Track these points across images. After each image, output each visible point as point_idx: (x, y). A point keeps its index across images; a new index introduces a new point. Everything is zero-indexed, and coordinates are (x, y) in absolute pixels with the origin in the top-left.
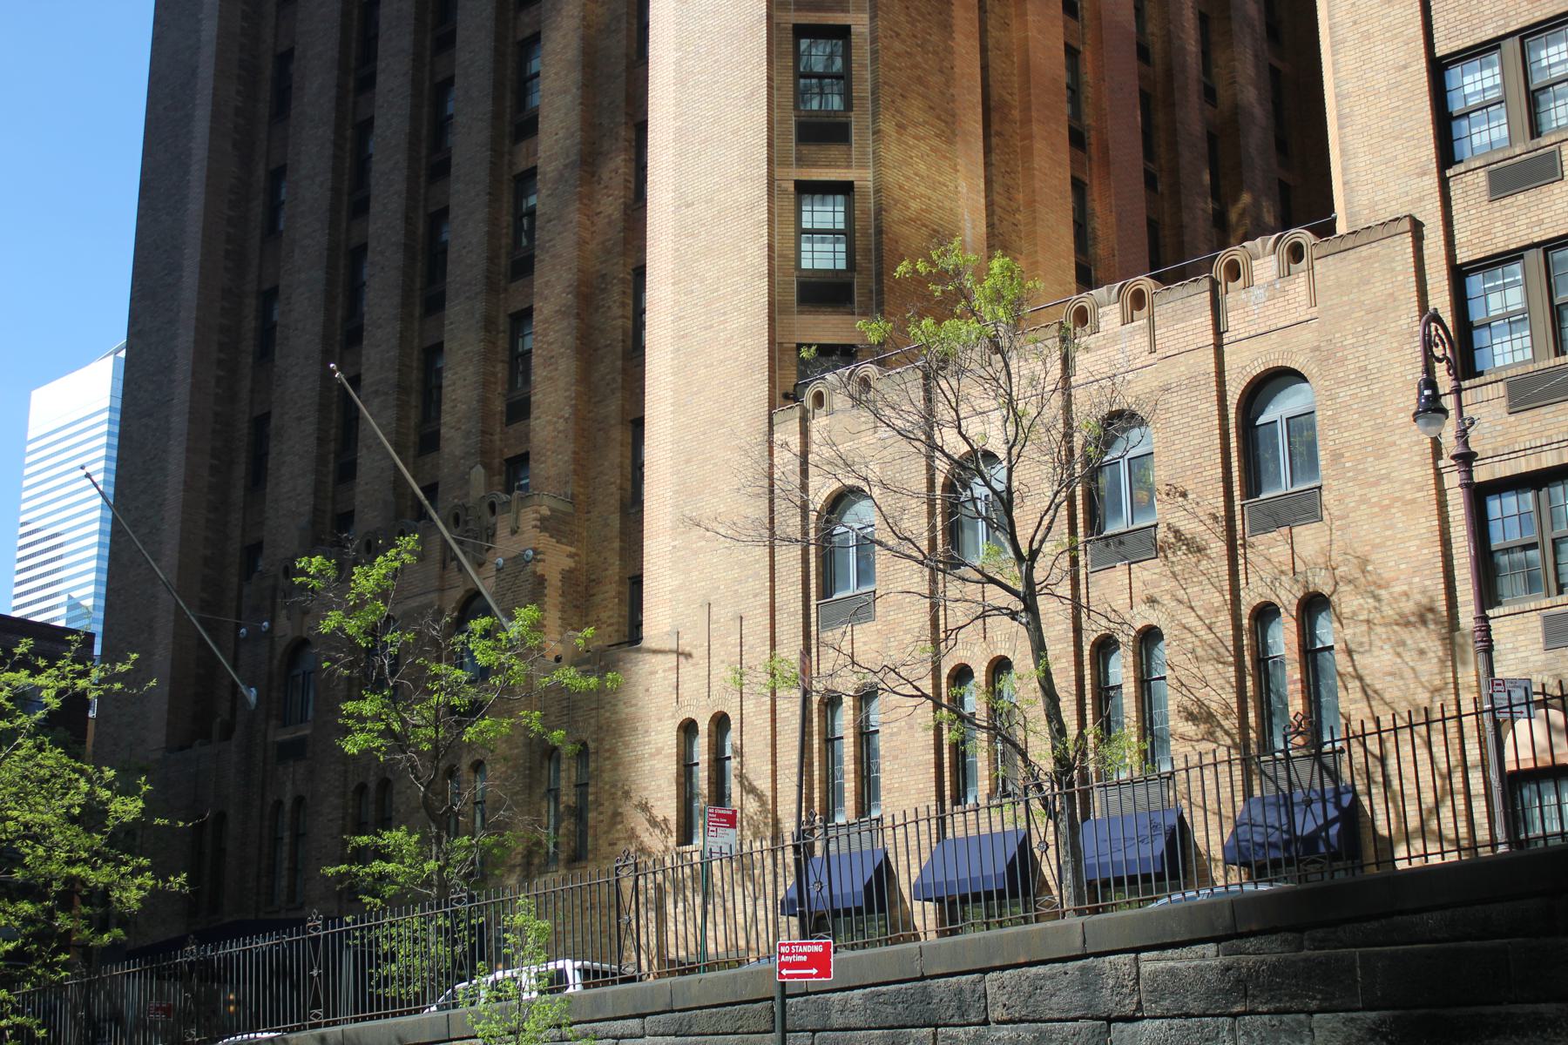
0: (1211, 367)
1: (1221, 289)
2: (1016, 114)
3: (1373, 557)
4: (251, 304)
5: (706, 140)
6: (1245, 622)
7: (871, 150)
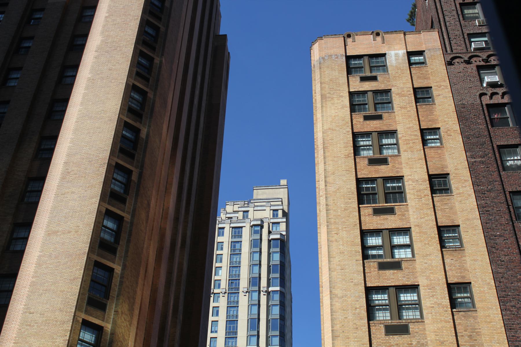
5: (46, 290)
7: (112, 317)
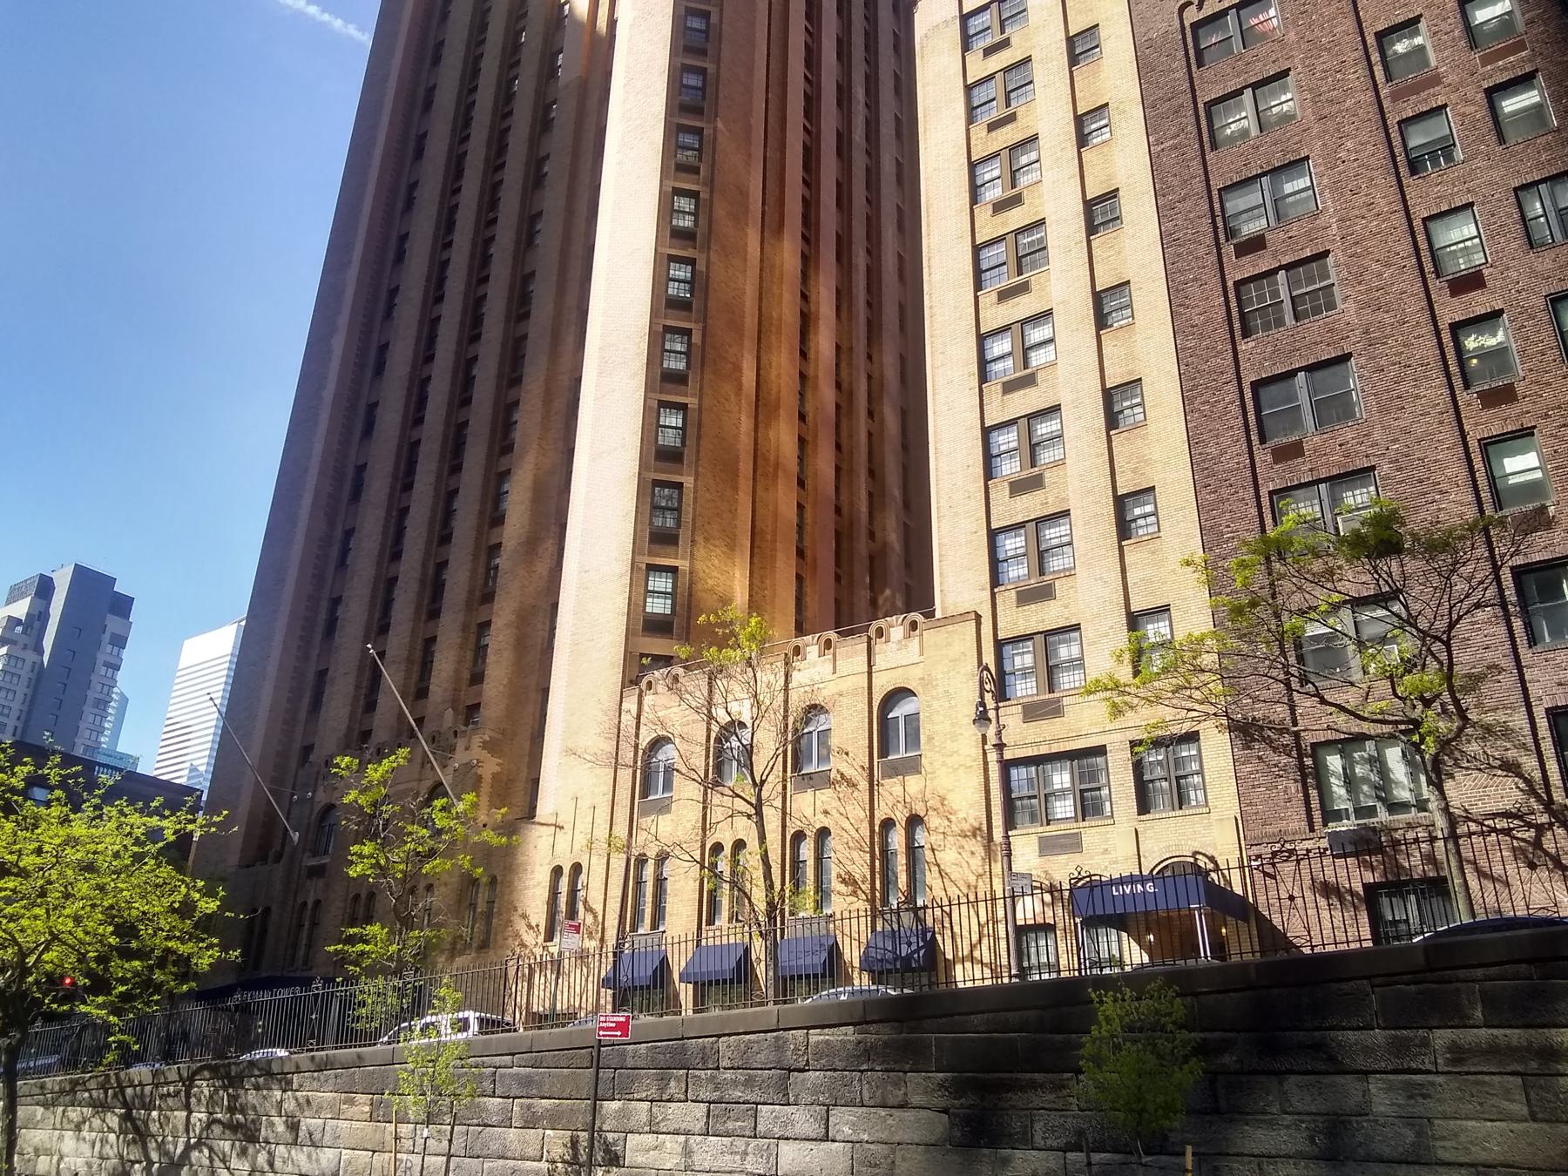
0: (866, 685)
1: (873, 642)
2: (769, 537)
3: (948, 797)
4: (324, 604)
6: (877, 829)
